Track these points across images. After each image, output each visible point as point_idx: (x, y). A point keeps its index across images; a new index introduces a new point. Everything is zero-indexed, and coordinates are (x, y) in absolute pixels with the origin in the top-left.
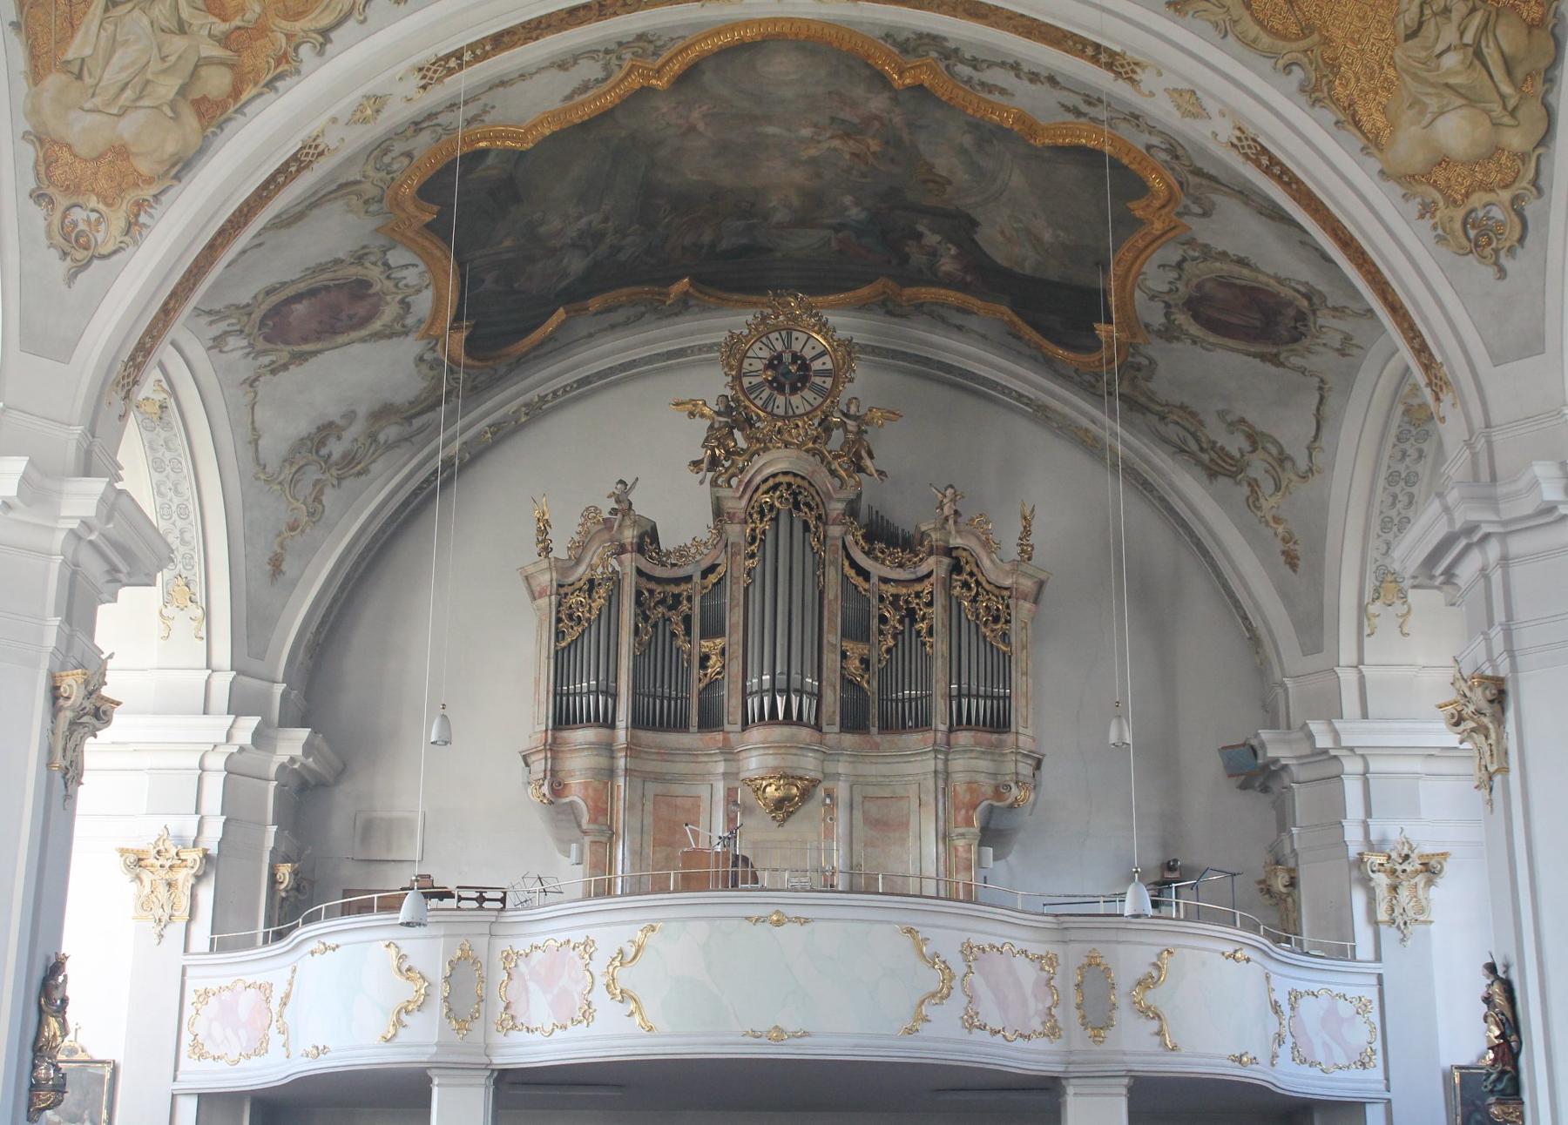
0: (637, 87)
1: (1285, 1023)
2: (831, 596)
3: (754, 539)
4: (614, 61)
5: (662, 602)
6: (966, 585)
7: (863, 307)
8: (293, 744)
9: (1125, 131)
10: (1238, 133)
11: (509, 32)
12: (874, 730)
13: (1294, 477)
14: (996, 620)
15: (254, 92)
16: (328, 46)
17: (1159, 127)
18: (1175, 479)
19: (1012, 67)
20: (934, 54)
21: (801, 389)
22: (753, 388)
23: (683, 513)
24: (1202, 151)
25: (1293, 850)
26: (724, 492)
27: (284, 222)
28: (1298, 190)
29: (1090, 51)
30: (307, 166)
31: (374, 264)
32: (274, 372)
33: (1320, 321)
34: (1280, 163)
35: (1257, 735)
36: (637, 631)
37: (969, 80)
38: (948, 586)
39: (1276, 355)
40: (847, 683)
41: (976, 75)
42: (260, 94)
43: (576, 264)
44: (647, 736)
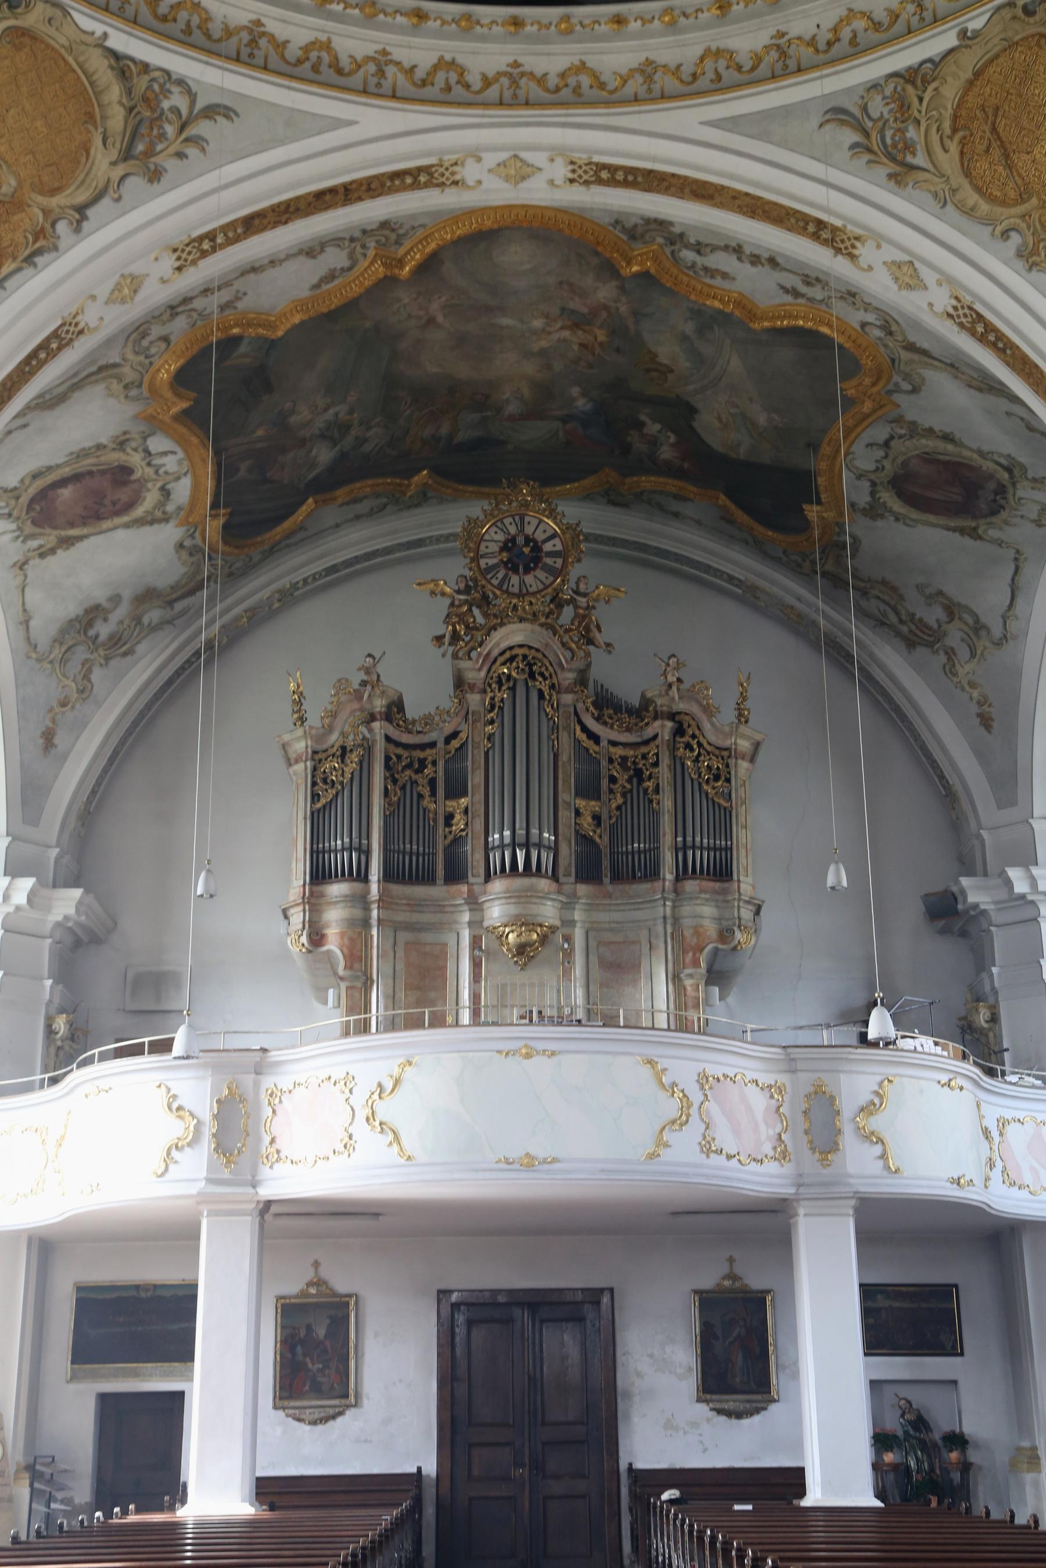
0: (381, 276)
1: (995, 1147)
4: (359, 249)
5: (409, 766)
6: (689, 747)
7: (588, 497)
8: (67, 903)
9: (840, 309)
10: (954, 302)
11: (260, 215)
12: (607, 880)
13: (988, 644)
14: (717, 778)
15: (13, 266)
16: (85, 224)
17: (874, 303)
18: (876, 651)
19: (734, 250)
20: (660, 240)
21: (534, 569)
22: (489, 569)
23: (424, 683)
24: (917, 326)
25: (993, 988)
26: (465, 664)
27: (49, 402)
28: (1013, 355)
29: (811, 228)
30: (68, 344)
31: (135, 450)
32: (42, 556)
33: (1020, 493)
34: (995, 330)
35: (957, 883)
37: (693, 266)
38: (673, 749)
39: (975, 529)
40: (583, 839)
41: (699, 260)
42: (19, 269)
43: (324, 455)
44: (397, 889)
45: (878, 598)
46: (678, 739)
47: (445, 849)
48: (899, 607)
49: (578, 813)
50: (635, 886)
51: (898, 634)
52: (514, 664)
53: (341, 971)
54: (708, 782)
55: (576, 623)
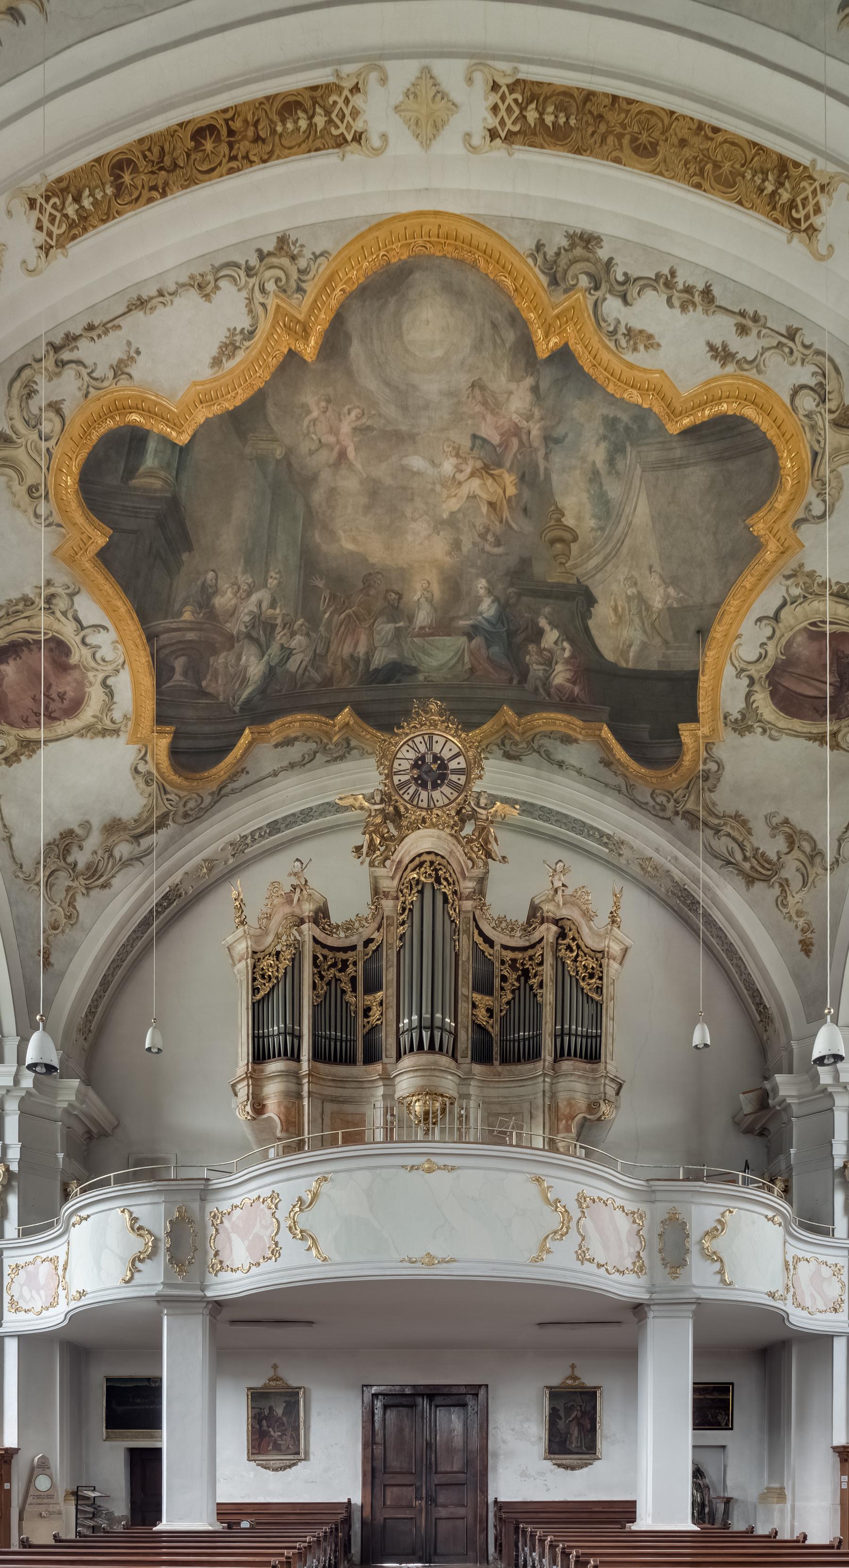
2: (464, 958)
3: (404, 909)
5: (334, 965)
6: (569, 948)
12: (496, 1063)
14: (591, 976)
21: (441, 785)
22: (402, 785)
26: (381, 872)
36: (315, 986)
38: (556, 949)
40: (479, 1028)
45: (729, 835)
46: (560, 942)
47: (364, 1037)
48: (746, 843)
49: (474, 1006)
50: (520, 1067)
51: (741, 872)
52: (423, 869)
53: (279, 1134)
54: (584, 979)
55: (477, 834)
